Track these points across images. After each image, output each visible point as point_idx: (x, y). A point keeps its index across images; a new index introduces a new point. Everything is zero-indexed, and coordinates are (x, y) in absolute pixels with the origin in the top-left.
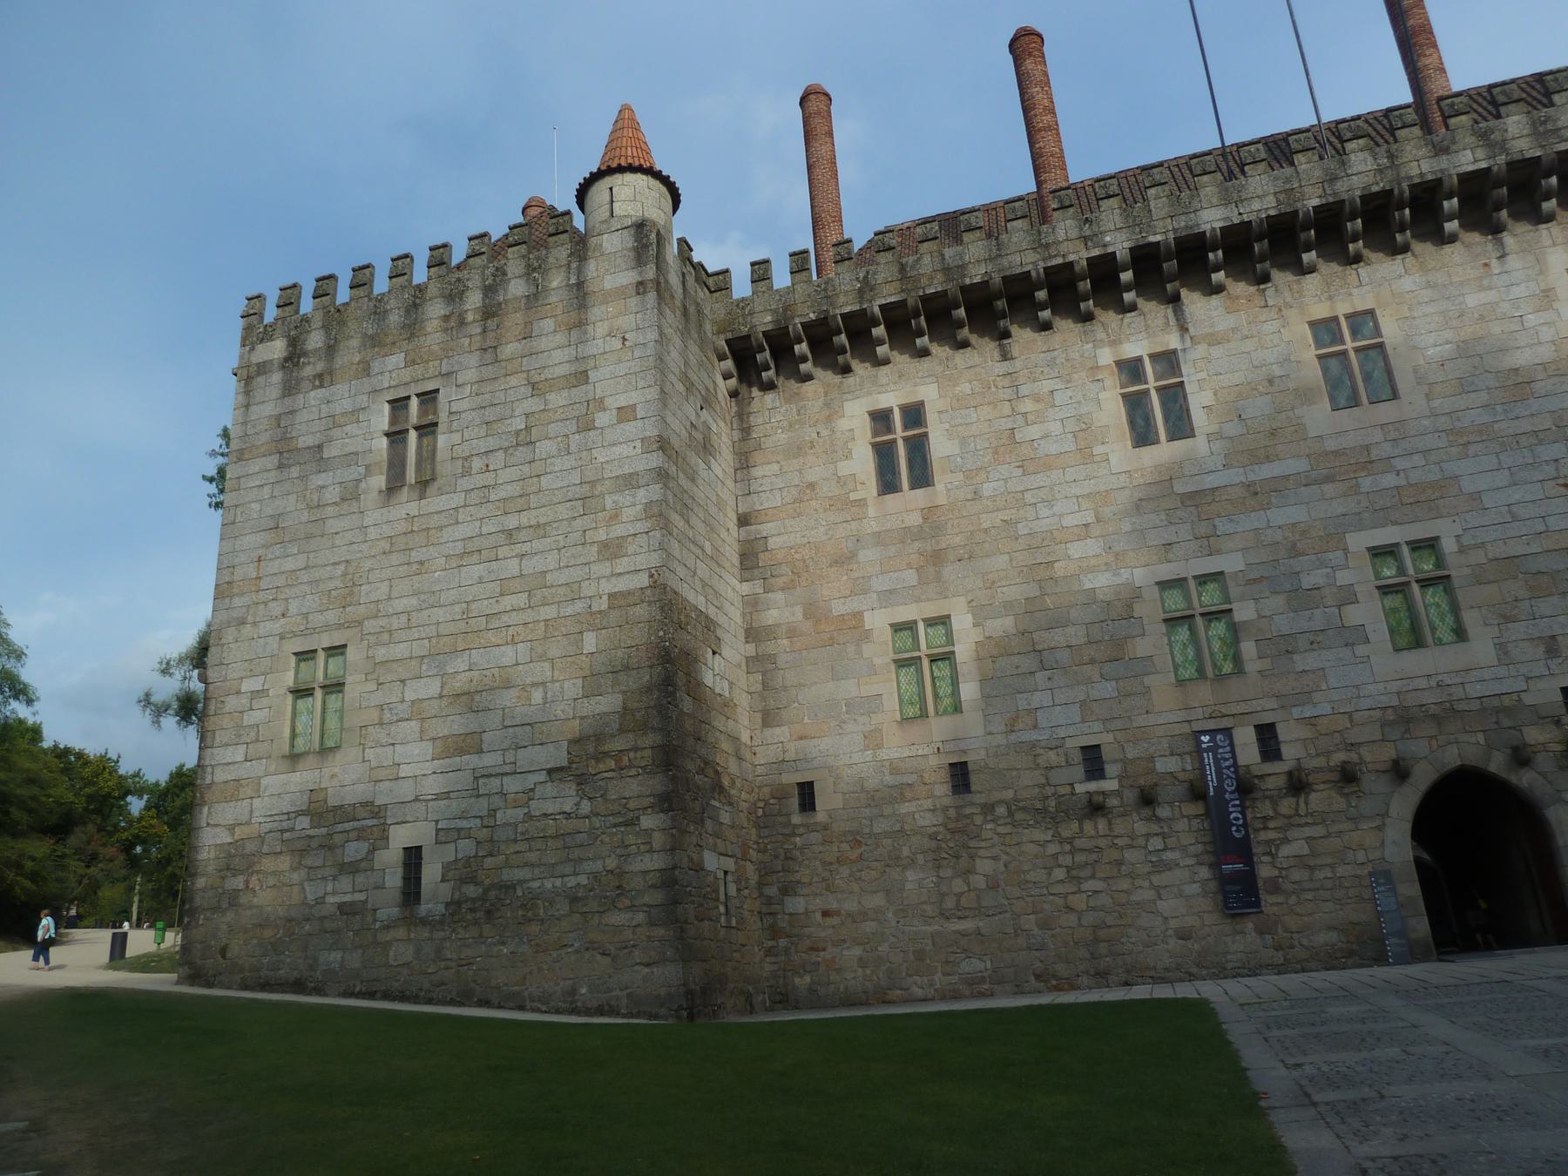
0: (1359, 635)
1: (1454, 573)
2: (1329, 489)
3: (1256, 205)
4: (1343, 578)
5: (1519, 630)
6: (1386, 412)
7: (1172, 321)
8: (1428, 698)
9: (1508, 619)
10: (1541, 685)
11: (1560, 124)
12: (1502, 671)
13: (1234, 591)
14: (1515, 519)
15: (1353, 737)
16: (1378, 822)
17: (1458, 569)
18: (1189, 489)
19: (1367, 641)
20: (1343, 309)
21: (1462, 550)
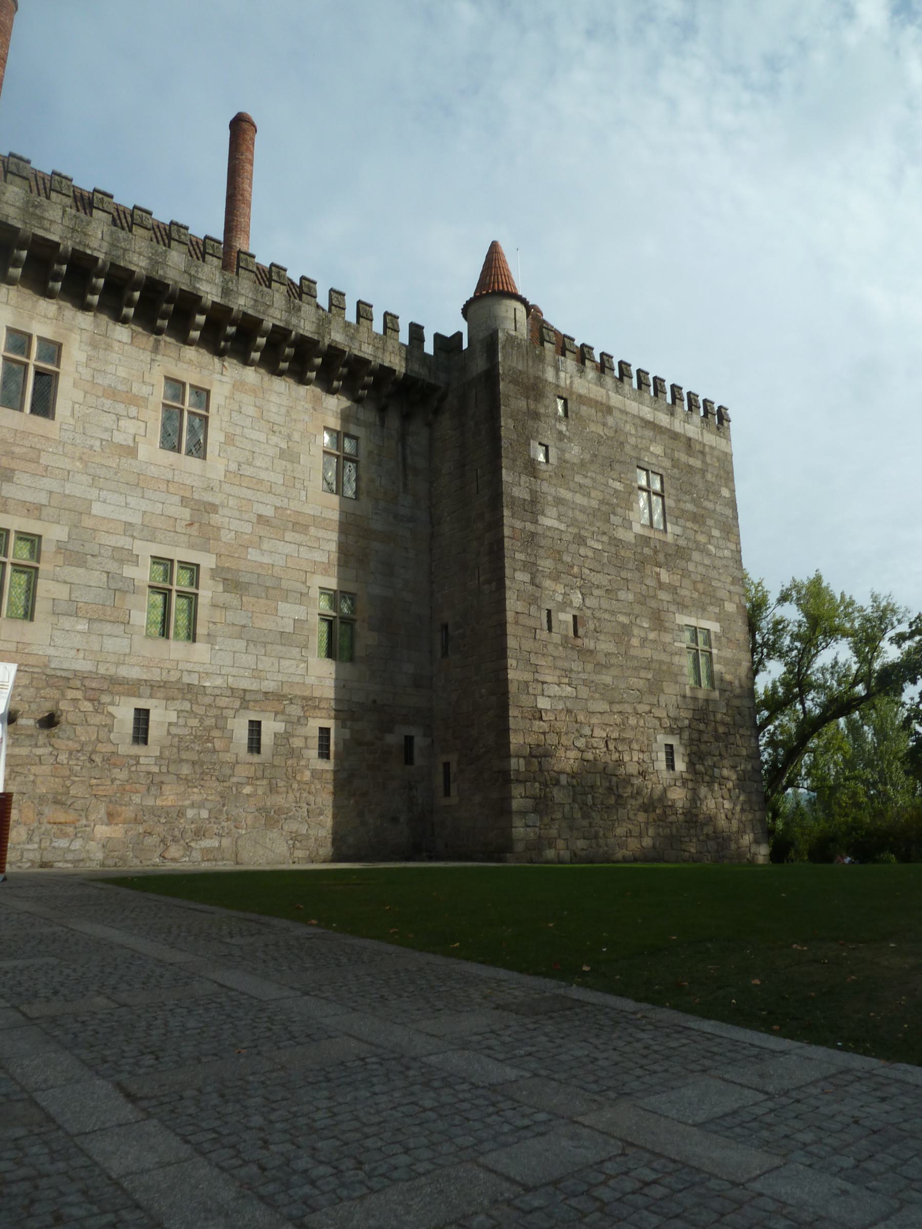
11: (46, 215)
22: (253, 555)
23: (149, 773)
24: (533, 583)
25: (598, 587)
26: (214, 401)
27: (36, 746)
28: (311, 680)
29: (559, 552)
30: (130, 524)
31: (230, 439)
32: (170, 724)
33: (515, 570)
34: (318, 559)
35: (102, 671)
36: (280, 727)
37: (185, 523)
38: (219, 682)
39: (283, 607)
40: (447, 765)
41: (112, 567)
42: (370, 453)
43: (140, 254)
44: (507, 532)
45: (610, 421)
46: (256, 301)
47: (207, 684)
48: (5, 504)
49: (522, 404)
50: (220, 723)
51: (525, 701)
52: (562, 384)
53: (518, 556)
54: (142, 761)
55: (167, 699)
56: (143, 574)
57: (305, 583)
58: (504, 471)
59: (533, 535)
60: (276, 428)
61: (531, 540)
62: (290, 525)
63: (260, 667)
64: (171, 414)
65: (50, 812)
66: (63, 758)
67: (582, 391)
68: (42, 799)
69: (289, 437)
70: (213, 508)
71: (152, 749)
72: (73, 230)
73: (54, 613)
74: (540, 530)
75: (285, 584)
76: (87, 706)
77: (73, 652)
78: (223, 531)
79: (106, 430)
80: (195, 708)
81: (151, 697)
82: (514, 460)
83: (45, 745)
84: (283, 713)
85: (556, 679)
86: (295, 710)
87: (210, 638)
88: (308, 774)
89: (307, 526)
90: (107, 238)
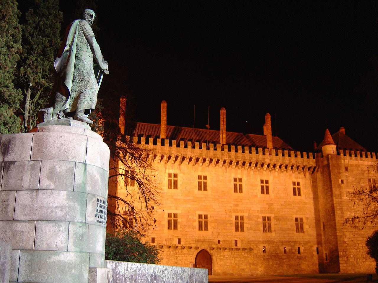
0: (194, 227)
1: (209, 220)
2: (195, 203)
3: (196, 154)
4: (195, 218)
5: (215, 230)
6: (205, 192)
7: (178, 168)
8: (202, 238)
9: (214, 229)
10: (215, 239)
12: (212, 236)
13: (178, 216)
14: (218, 214)
15: (191, 242)
16: (191, 256)
17: (209, 219)
18: (176, 198)
19: (196, 228)
20: (203, 174)
21: (211, 217)
22: (281, 213)
23: (266, 258)
24: (342, 213)
25: (359, 211)
26: (270, 182)
27: (248, 254)
28: (295, 237)
29: (348, 204)
30: (258, 211)
31: (274, 189)
32: (269, 249)
33: (337, 211)
34: (294, 211)
35: (257, 240)
36: (290, 248)
37: (267, 209)
38: (277, 240)
39: (288, 222)
40: (326, 254)
41: (256, 220)
42: (303, 185)
43: (254, 157)
44: (335, 202)
45: (360, 169)
46: (276, 160)
47: (275, 240)
48: (238, 211)
49: (336, 171)
50: (278, 247)
51: (341, 239)
52: (346, 163)
53: (338, 207)
54: (265, 256)
55: (269, 244)
56: (261, 220)
57: (292, 217)
58: (333, 189)
59: (341, 202)
60: (283, 184)
61: (341, 203)
62: (288, 205)
63: (285, 235)
64: (262, 187)
65: (252, 266)
66: (252, 256)
67: (351, 163)
68: (250, 263)
69: (285, 185)
70: (272, 204)
71: (267, 254)
72: (243, 157)
73: (248, 230)
74: (343, 200)
75: (288, 218)
76: (255, 247)
77: (252, 237)
78: (275, 209)
79: (251, 193)
80: (273, 245)
81: (266, 244)
82: (335, 185)
83: (249, 254)
84: (290, 245)
85: (348, 234)
86: (292, 244)
87: (275, 231)
88: (296, 257)
89: (291, 204)
90: (249, 156)
